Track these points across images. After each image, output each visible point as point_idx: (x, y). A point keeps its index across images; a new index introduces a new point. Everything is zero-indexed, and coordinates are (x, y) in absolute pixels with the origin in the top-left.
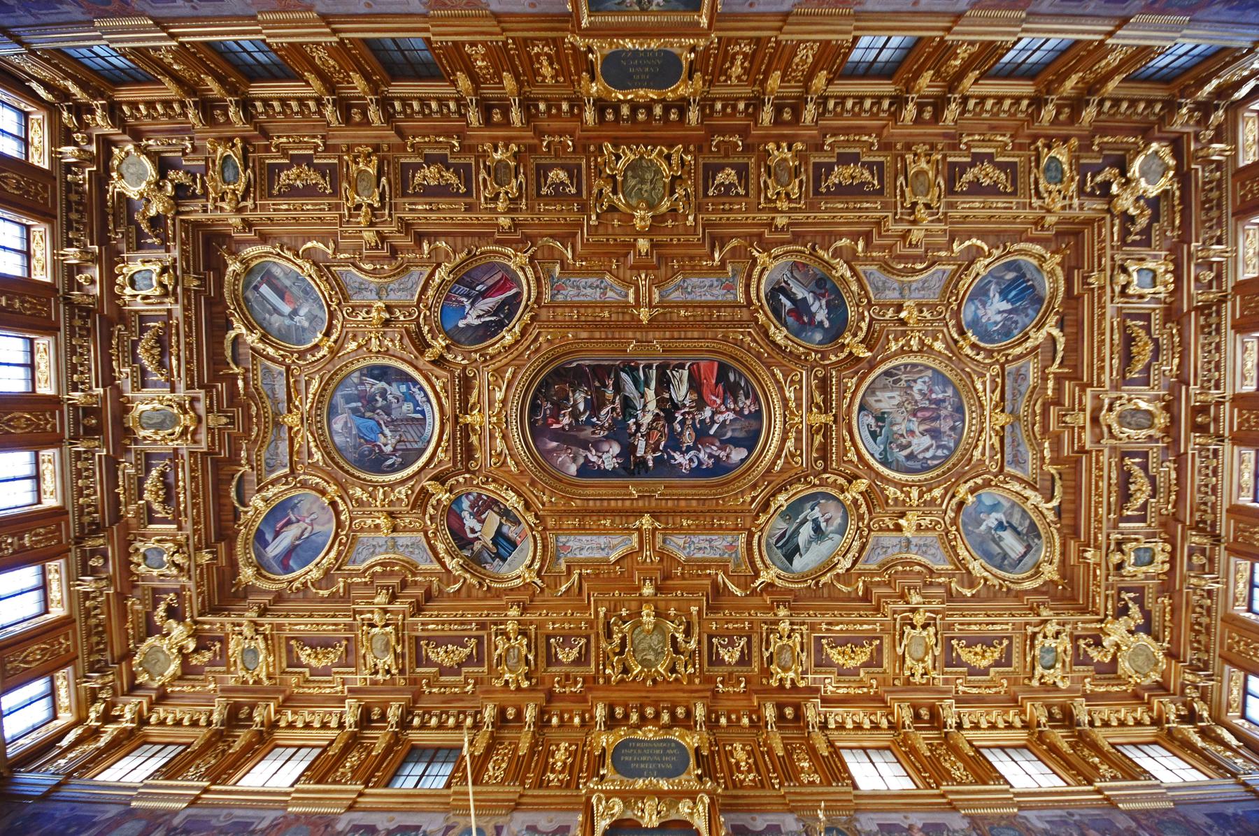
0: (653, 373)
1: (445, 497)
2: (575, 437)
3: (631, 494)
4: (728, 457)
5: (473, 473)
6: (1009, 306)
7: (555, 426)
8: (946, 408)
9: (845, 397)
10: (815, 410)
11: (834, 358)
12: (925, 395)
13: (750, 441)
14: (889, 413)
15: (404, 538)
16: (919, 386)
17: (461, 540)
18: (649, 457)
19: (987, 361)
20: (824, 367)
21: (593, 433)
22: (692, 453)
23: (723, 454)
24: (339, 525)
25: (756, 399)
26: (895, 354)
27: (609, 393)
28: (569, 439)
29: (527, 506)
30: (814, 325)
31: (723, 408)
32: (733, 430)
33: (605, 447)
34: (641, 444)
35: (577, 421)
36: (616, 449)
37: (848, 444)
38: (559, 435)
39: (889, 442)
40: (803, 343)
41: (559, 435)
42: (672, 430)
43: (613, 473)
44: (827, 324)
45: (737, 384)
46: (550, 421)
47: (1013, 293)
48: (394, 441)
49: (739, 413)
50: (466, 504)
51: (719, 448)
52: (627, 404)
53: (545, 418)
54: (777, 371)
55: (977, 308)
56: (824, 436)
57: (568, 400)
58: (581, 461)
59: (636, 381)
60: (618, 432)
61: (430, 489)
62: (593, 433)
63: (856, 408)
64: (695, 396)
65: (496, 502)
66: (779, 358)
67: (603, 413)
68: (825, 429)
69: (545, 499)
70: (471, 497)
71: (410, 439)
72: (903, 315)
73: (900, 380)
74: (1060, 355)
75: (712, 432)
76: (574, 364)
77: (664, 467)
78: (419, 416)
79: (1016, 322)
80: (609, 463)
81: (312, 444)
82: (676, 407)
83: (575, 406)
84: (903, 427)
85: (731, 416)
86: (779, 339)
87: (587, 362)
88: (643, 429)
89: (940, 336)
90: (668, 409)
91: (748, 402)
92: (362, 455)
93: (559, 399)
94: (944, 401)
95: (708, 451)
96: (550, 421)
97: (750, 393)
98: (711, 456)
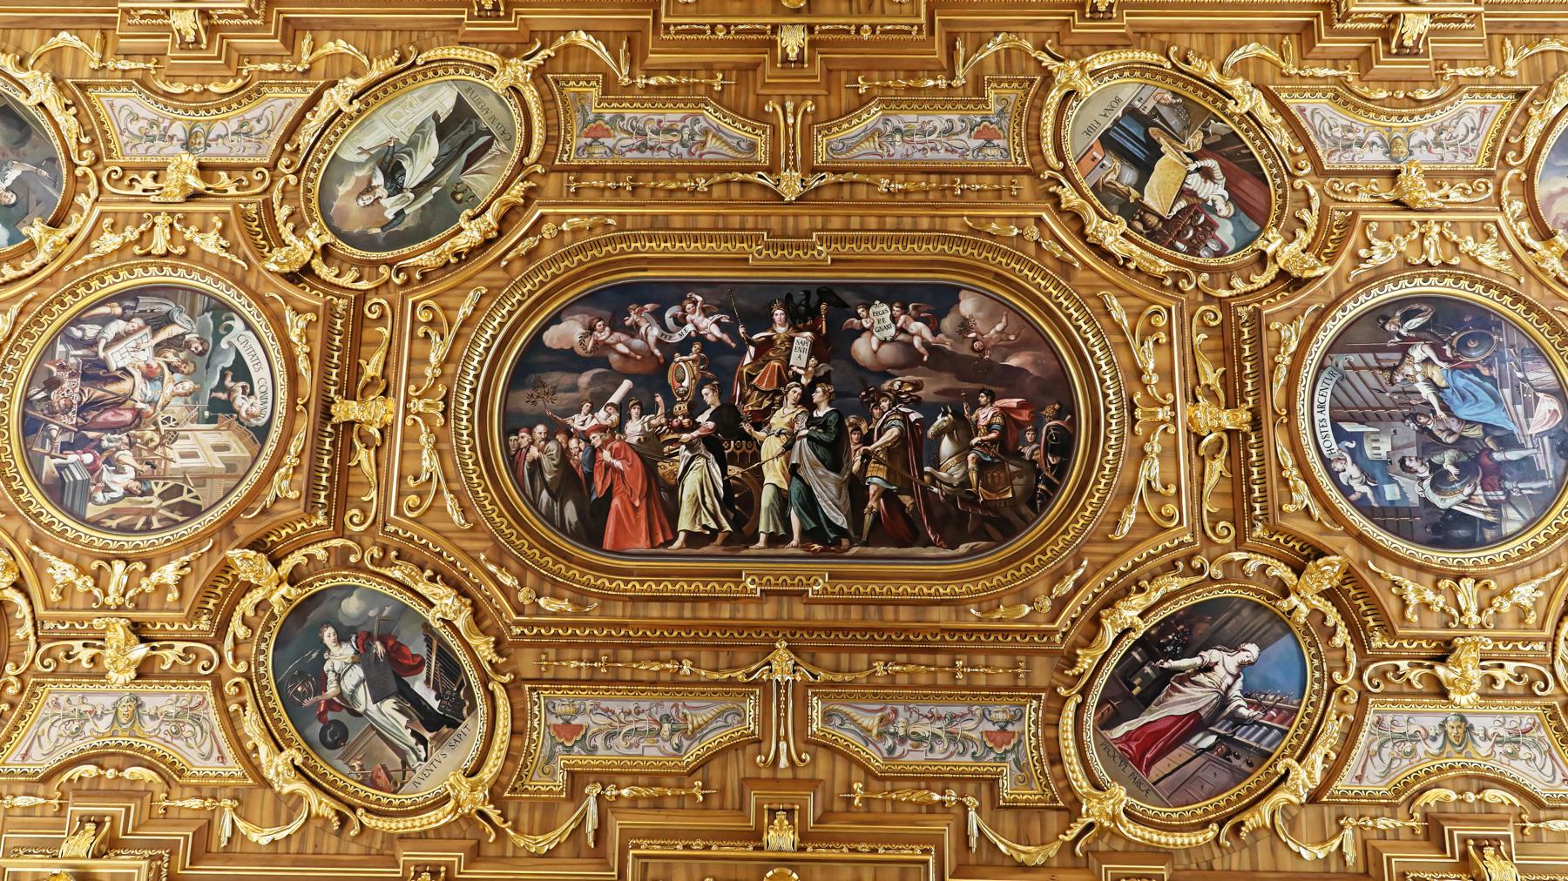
0: (763, 526)
1: (1272, 242)
2: (962, 378)
3: (829, 241)
4: (591, 329)
5: (1209, 298)
7: (1013, 402)
8: (64, 430)
10: (374, 430)
11: (318, 551)
12: (108, 462)
13: (535, 363)
15: (1374, 157)
16: (120, 483)
17: (1234, 157)
18: (781, 330)
20: (340, 532)
21: (917, 386)
22: (677, 338)
23: (603, 335)
24: (1527, 188)
25: (513, 461)
27: (876, 479)
28: (984, 374)
29: (1076, 221)
30: (356, 634)
31: (596, 440)
32: (574, 388)
33: (887, 352)
34: (799, 359)
35: (958, 414)
36: (862, 348)
37: (301, 350)
38: (1002, 380)
39: (207, 355)
40: (393, 592)
41: (1002, 380)
42: (723, 391)
43: (869, 294)
44: (329, 635)
46: (1025, 416)
48: (1408, 370)
49: (557, 428)
50: (1226, 232)
51: (610, 347)
52: (832, 452)
53: (1037, 422)
54: (457, 517)
56: (359, 371)
57: (980, 463)
58: (947, 323)
59: (810, 504)
60: (857, 388)
61: (1310, 258)
62: (917, 386)
63: (274, 436)
64: (664, 468)
65: (1152, 234)
66: (451, 554)
67: (892, 433)
69: (1033, 232)
70: (1213, 246)
71: (1367, 375)
72: (141, 651)
73: (160, 496)
75: (626, 384)
76: (963, 548)
77: (746, 306)
78: (1349, 427)
80: (880, 315)
82: (711, 443)
83: (962, 450)
85: (576, 422)
86: (445, 601)
87: (930, 552)
88: (794, 393)
89: (54, 597)
90: (731, 439)
91: (534, 452)
92: (1483, 339)
93: (1002, 466)
94: (66, 447)
95: (637, 343)
96: (1025, 416)
97: (527, 473)
98: (633, 331)
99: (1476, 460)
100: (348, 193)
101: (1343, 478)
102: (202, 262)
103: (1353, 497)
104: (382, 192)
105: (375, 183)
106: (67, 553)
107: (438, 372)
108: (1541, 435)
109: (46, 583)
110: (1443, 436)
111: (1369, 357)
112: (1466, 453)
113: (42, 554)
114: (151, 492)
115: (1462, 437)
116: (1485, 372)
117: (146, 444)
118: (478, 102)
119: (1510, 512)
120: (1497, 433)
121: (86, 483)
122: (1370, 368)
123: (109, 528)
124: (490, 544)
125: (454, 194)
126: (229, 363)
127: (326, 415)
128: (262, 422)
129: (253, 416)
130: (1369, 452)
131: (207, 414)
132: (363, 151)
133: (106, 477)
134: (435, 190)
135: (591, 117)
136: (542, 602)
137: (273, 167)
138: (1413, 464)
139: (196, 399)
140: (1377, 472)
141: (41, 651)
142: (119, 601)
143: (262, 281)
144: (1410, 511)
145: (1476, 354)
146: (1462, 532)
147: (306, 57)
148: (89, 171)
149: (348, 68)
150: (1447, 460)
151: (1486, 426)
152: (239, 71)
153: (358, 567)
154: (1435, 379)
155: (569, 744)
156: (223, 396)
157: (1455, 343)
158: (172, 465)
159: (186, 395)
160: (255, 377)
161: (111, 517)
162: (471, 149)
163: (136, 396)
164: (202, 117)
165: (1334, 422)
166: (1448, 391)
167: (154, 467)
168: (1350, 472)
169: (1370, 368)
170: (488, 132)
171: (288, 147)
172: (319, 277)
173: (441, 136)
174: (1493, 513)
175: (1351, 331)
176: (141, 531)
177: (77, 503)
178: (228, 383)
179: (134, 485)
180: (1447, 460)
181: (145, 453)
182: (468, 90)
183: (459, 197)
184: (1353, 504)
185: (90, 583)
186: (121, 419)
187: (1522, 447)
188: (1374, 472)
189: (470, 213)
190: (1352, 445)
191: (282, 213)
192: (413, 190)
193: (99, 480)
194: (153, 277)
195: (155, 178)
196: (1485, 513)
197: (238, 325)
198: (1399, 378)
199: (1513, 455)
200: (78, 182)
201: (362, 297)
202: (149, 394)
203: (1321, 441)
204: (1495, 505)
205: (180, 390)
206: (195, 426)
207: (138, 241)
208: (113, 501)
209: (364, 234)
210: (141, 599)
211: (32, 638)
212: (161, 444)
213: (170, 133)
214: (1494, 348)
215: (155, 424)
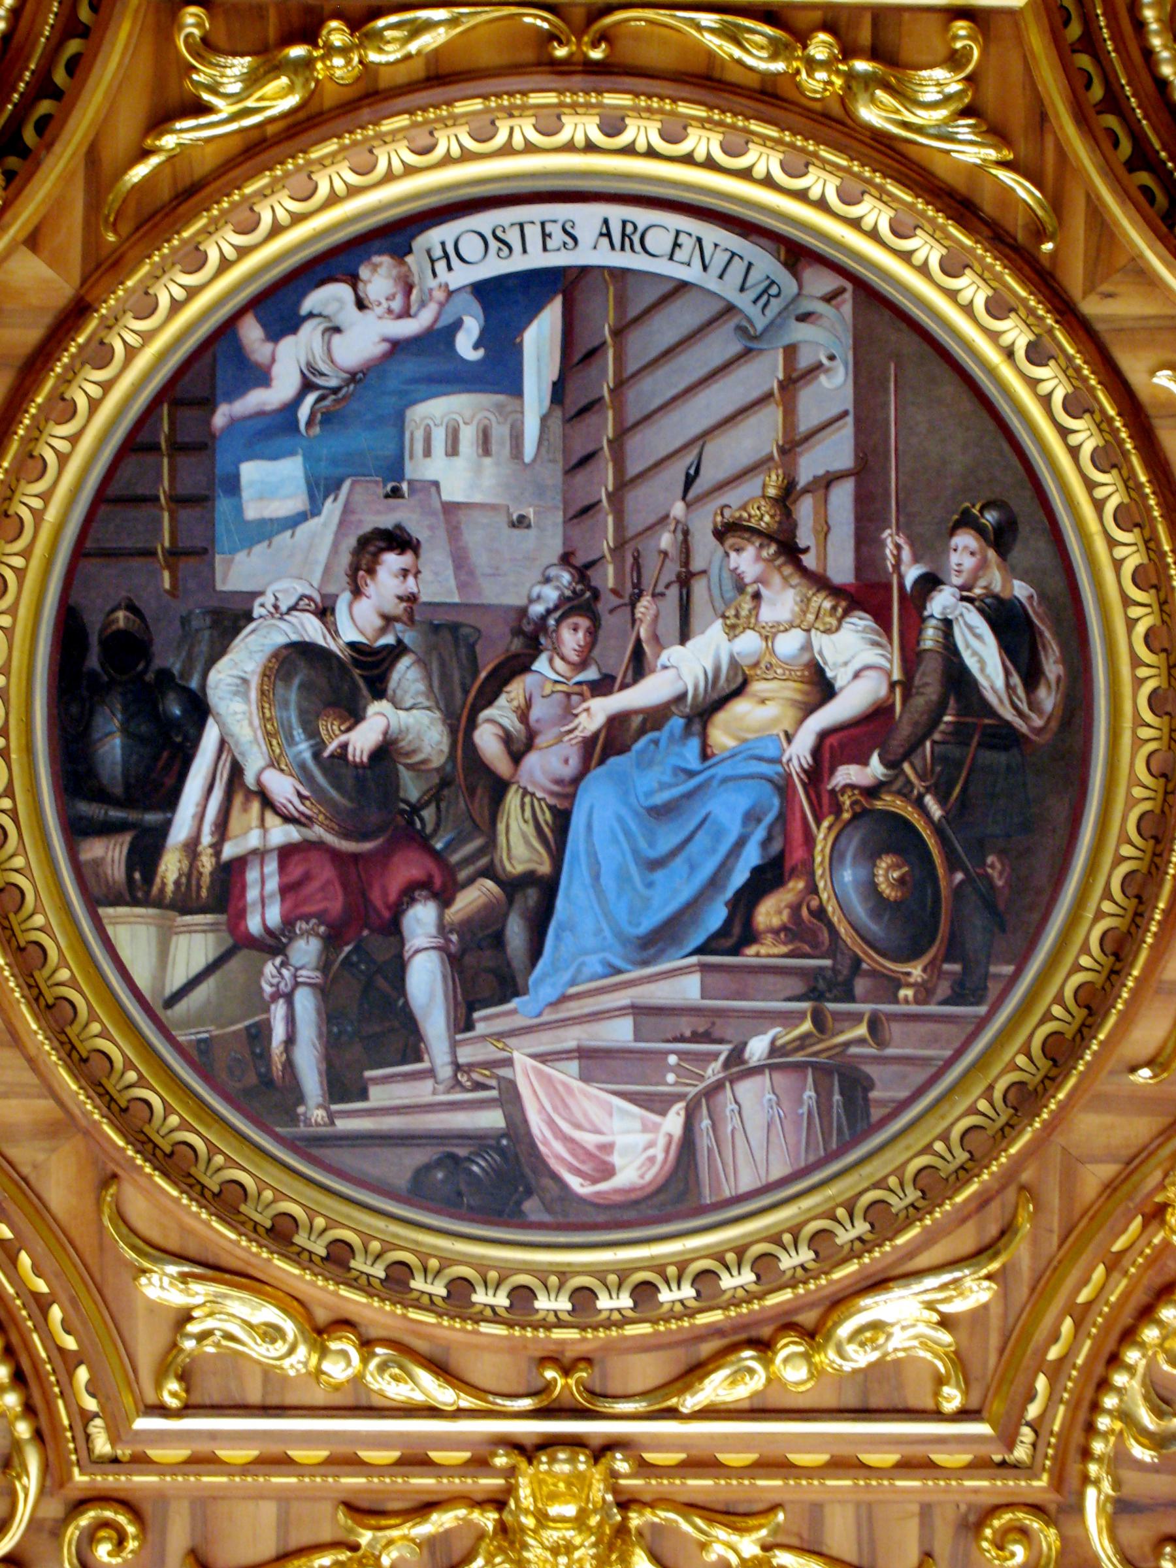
48: (782, 601)
71: (760, 435)
78: (541, 339)
81: (791, 1368)
92: (914, 922)
99: (406, 831)
101: (330, 297)
103: (251, 332)
108: (510, 1098)
110: (501, 712)
111: (835, 452)
112: (435, 797)
115: (499, 788)
116: (770, 912)
119: (194, 948)
120: (516, 932)
122: (791, 447)
130: (435, 412)
138: (389, 578)
140: (359, 439)
144: (194, 554)
145: (846, 883)
146: (112, 748)
150: (404, 717)
151: (548, 887)
154: (740, 707)
157: (890, 802)
165: (565, 283)
166: (690, 753)
168: (354, 329)
169: (791, 447)
174: (191, 873)
175: (950, 388)
180: (404, 717)
184: (227, 329)
187: (462, 1022)
188: (357, 418)
190: (466, 345)
196: (191, 847)
198: (747, 561)
199: (426, 981)
203: (484, 221)
204: (223, 890)
214: (871, 960)
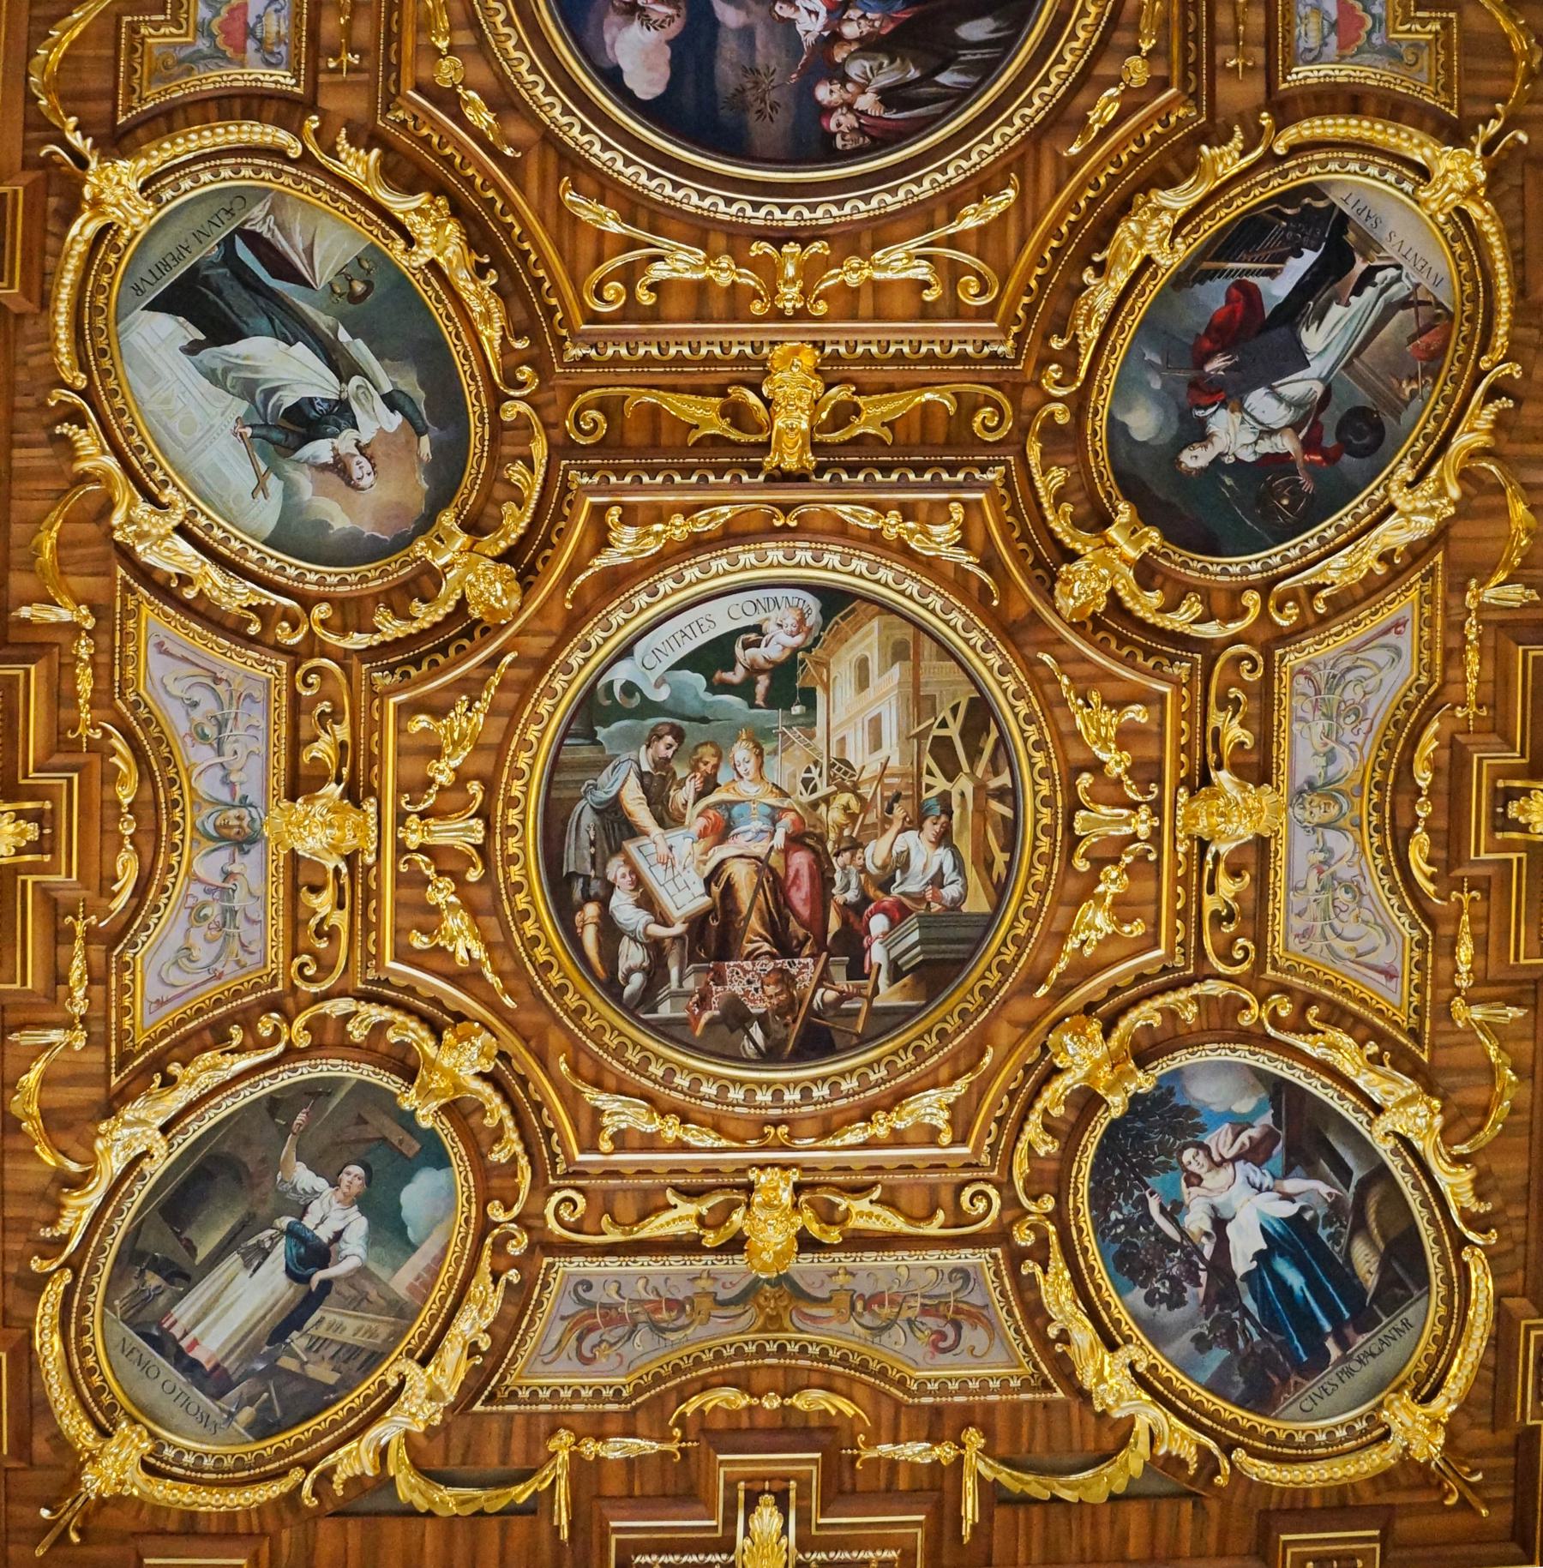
6: (1242, 1264)
9: (881, 508)
12: (885, 885)
14: (809, 721)
19: (1021, 1168)
26: (1068, 736)
37: (679, 528)
39: (679, 723)
40: (1122, 341)
45: (946, 53)
47: (1295, 1280)
54: (996, 205)
55: (1240, 1125)
68: (741, 451)
74: (1034, 1486)
79: (1175, 1300)
84: (748, 789)
100: (348, 510)
102: (500, 750)
104: (346, 441)
105: (327, 458)
106: (1056, 926)
107: (725, 261)
109: (1112, 952)
113: (1062, 966)
114: (945, 797)
117: (853, 817)
118: (164, 266)
121: (926, 923)
123: (1009, 865)
124: (1046, 143)
125: (353, 298)
126: (698, 680)
127: (798, 478)
128: (813, 603)
129: (802, 621)
131: (797, 710)
132: (261, 486)
133: (913, 887)
134: (344, 336)
135: (203, 44)
136: (1146, 47)
137: (295, 656)
139: (768, 734)
141: (1221, 968)
142: (1144, 812)
143: (538, 625)
147: (65, 615)
148: (299, 1022)
149: (91, 529)
152: (93, 747)
153: (1079, 404)
155: (1369, 23)
156: (763, 682)
158: (895, 763)
159: (760, 755)
160: (724, 627)
161: (989, 866)
162: (262, 274)
163: (760, 849)
164: (189, 817)
167: (897, 797)
170: (228, 242)
171: (254, 629)
172: (522, 538)
173: (236, 335)
176: (1015, 809)
177: (962, 932)
178: (736, 676)
179: (931, 829)
181: (872, 818)
182: (138, 290)
183: (359, 287)
185: (1112, 871)
186: (805, 872)
189: (401, 244)
191: (392, 628)
192: (343, 379)
193: (919, 898)
194: (526, 844)
195: (316, 890)
197: (621, 673)
200: (328, 1038)
201: (561, 449)
202: (758, 825)
205: (751, 766)
206: (820, 729)
207: (458, 878)
208: (959, 867)
209: (431, 469)
210: (1141, 776)
211: (1197, 989)
212: (854, 789)
213: (218, 881)
215: (814, 805)
